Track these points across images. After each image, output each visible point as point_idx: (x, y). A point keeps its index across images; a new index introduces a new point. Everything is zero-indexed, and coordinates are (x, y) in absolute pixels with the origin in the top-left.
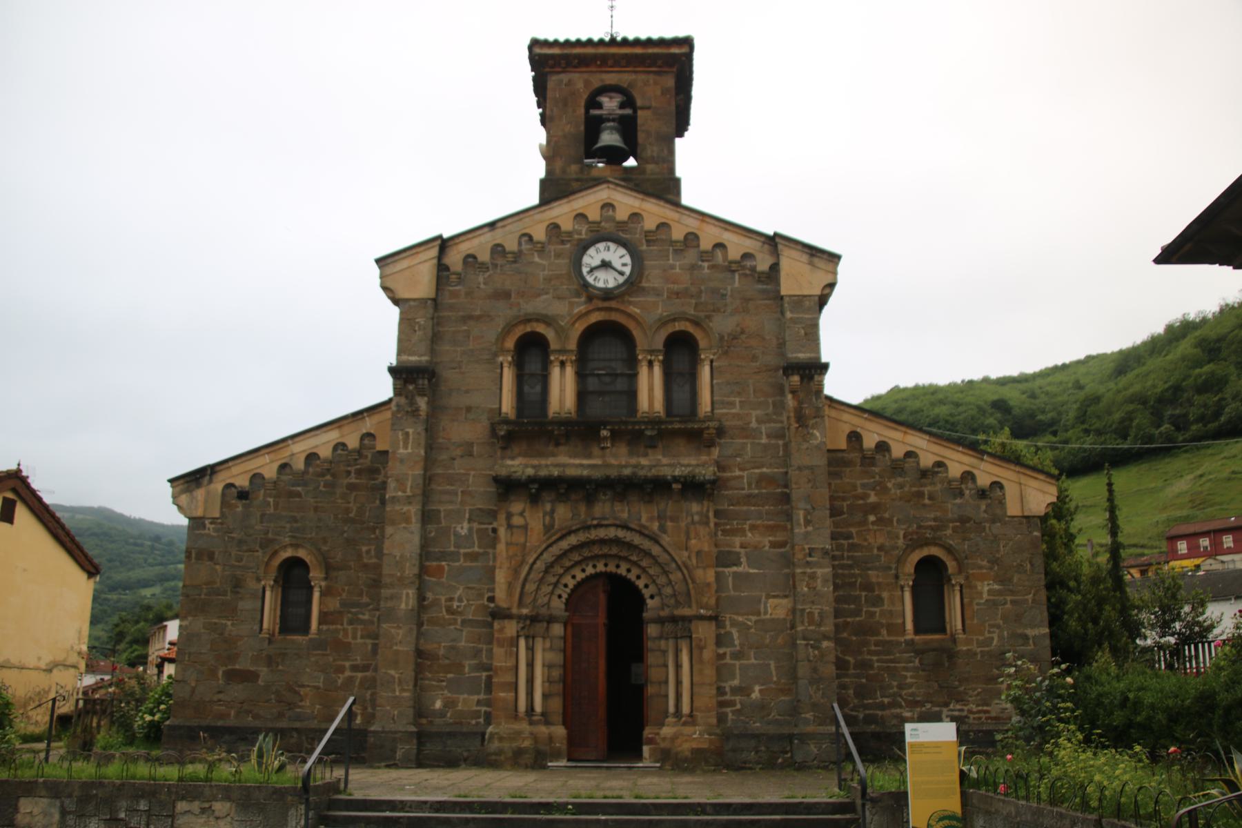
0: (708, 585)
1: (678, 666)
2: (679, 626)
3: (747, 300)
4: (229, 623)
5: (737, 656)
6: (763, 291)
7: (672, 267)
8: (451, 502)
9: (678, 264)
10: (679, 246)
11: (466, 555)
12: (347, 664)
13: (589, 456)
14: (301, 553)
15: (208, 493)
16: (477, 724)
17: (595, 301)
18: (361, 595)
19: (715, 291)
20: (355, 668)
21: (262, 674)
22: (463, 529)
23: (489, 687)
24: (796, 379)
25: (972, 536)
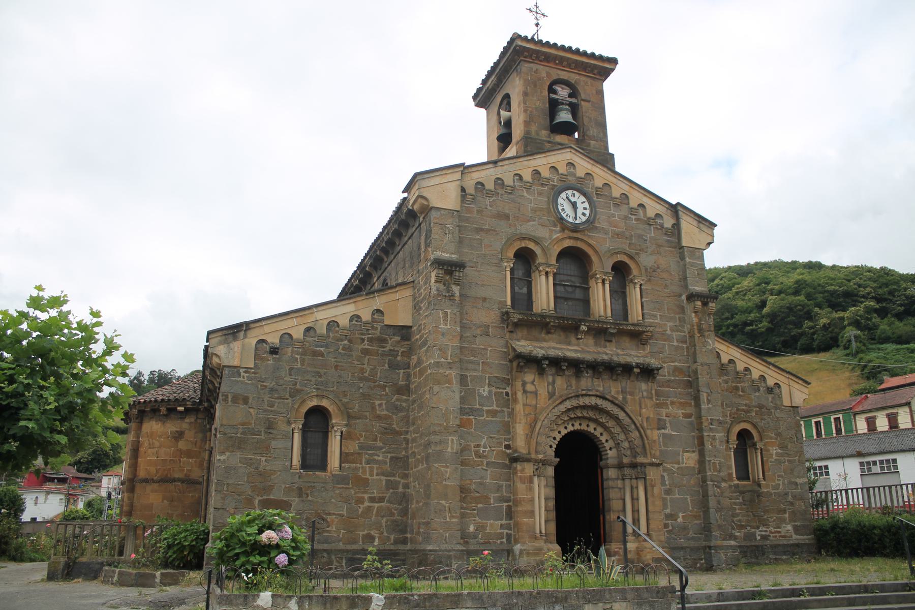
0: (655, 441)
1: (634, 499)
2: (635, 469)
3: (660, 246)
4: (263, 459)
5: (668, 492)
6: (668, 241)
7: (614, 216)
8: (476, 370)
9: (618, 214)
10: (617, 202)
11: (488, 411)
12: (366, 496)
13: (569, 344)
14: (325, 403)
15: (243, 346)
16: (502, 543)
17: (566, 231)
18: (376, 440)
19: (640, 237)
20: (372, 500)
21: (294, 504)
22: (485, 391)
23: (510, 514)
24: (699, 303)
25: (765, 417)
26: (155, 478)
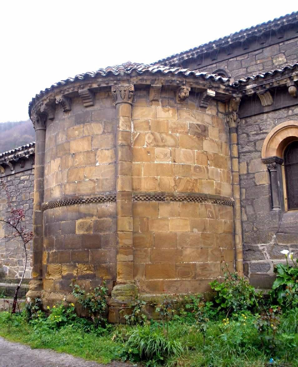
26: (176, 192)
